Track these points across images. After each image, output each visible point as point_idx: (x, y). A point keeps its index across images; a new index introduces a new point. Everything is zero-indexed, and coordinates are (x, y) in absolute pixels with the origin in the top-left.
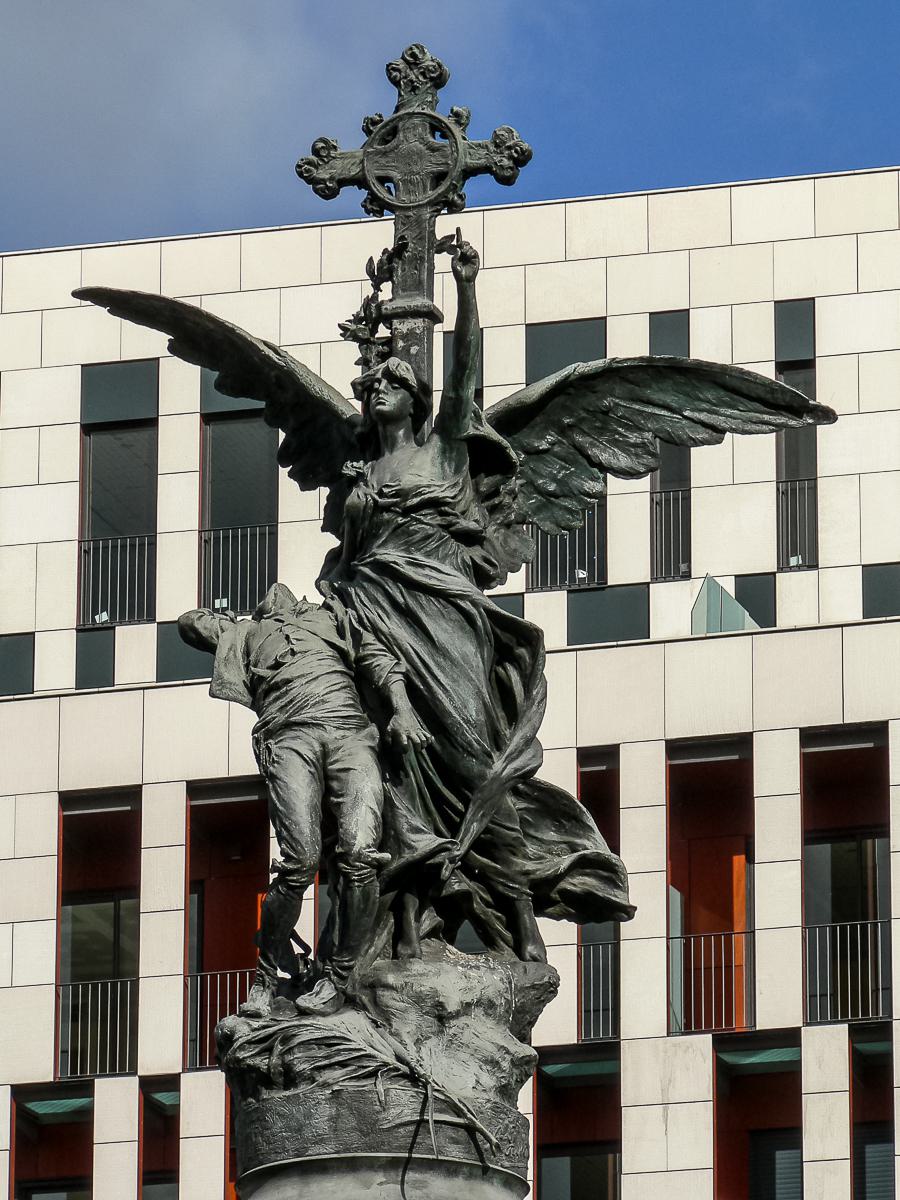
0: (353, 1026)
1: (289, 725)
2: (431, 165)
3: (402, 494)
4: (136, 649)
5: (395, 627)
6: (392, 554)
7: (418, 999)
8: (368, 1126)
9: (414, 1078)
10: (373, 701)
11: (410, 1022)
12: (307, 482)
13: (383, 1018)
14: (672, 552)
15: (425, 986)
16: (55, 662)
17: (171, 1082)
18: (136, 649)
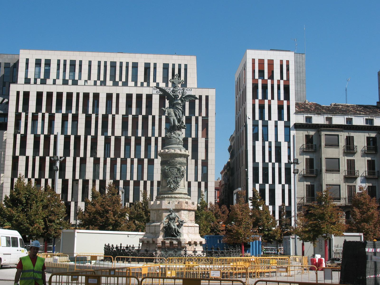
0: (174, 135)
1: (171, 116)
2: (178, 81)
3: (178, 103)
4: (39, 81)
5: (177, 111)
6: (177, 106)
7: (178, 134)
8: (176, 142)
9: (179, 139)
10: (176, 115)
11: (178, 135)
12: (168, 100)
13: (176, 135)
14: (80, 78)
15: (178, 133)
16: (32, 81)
17: (44, 114)
18: (39, 81)
